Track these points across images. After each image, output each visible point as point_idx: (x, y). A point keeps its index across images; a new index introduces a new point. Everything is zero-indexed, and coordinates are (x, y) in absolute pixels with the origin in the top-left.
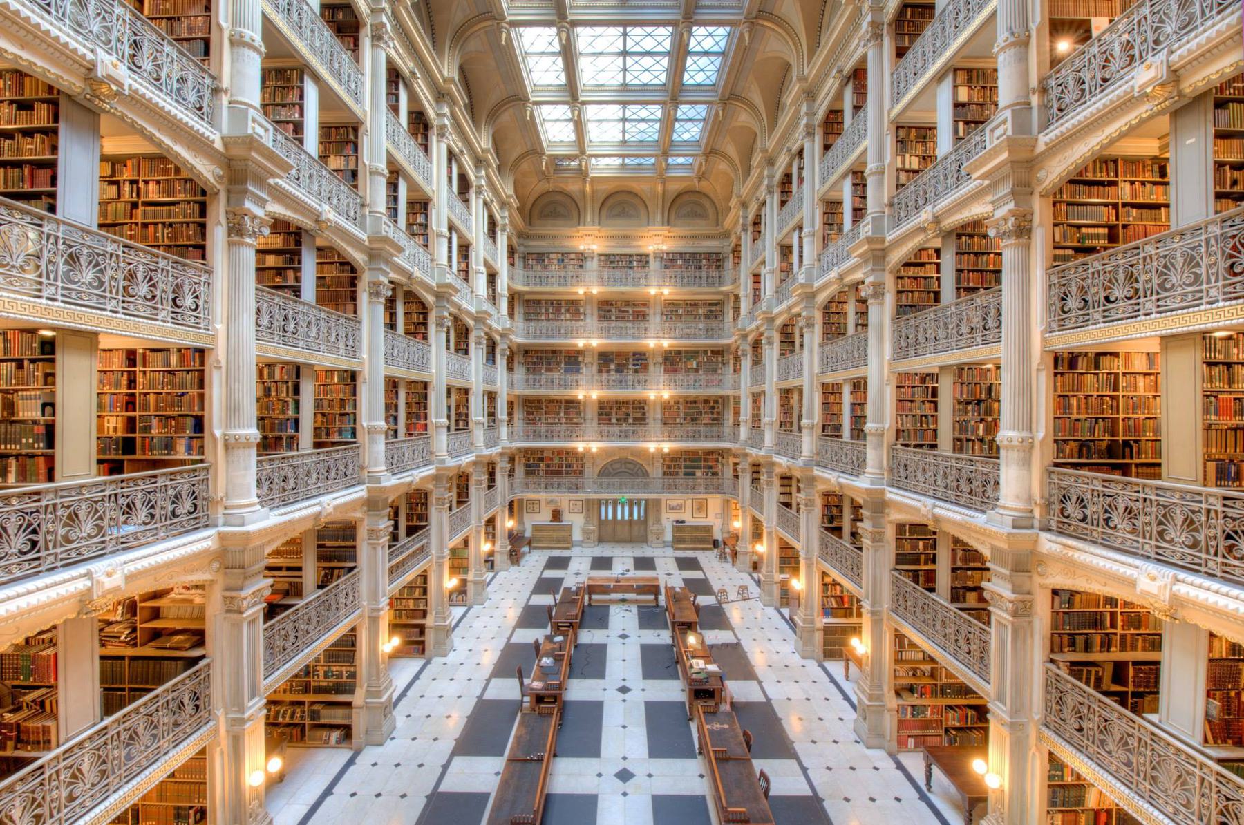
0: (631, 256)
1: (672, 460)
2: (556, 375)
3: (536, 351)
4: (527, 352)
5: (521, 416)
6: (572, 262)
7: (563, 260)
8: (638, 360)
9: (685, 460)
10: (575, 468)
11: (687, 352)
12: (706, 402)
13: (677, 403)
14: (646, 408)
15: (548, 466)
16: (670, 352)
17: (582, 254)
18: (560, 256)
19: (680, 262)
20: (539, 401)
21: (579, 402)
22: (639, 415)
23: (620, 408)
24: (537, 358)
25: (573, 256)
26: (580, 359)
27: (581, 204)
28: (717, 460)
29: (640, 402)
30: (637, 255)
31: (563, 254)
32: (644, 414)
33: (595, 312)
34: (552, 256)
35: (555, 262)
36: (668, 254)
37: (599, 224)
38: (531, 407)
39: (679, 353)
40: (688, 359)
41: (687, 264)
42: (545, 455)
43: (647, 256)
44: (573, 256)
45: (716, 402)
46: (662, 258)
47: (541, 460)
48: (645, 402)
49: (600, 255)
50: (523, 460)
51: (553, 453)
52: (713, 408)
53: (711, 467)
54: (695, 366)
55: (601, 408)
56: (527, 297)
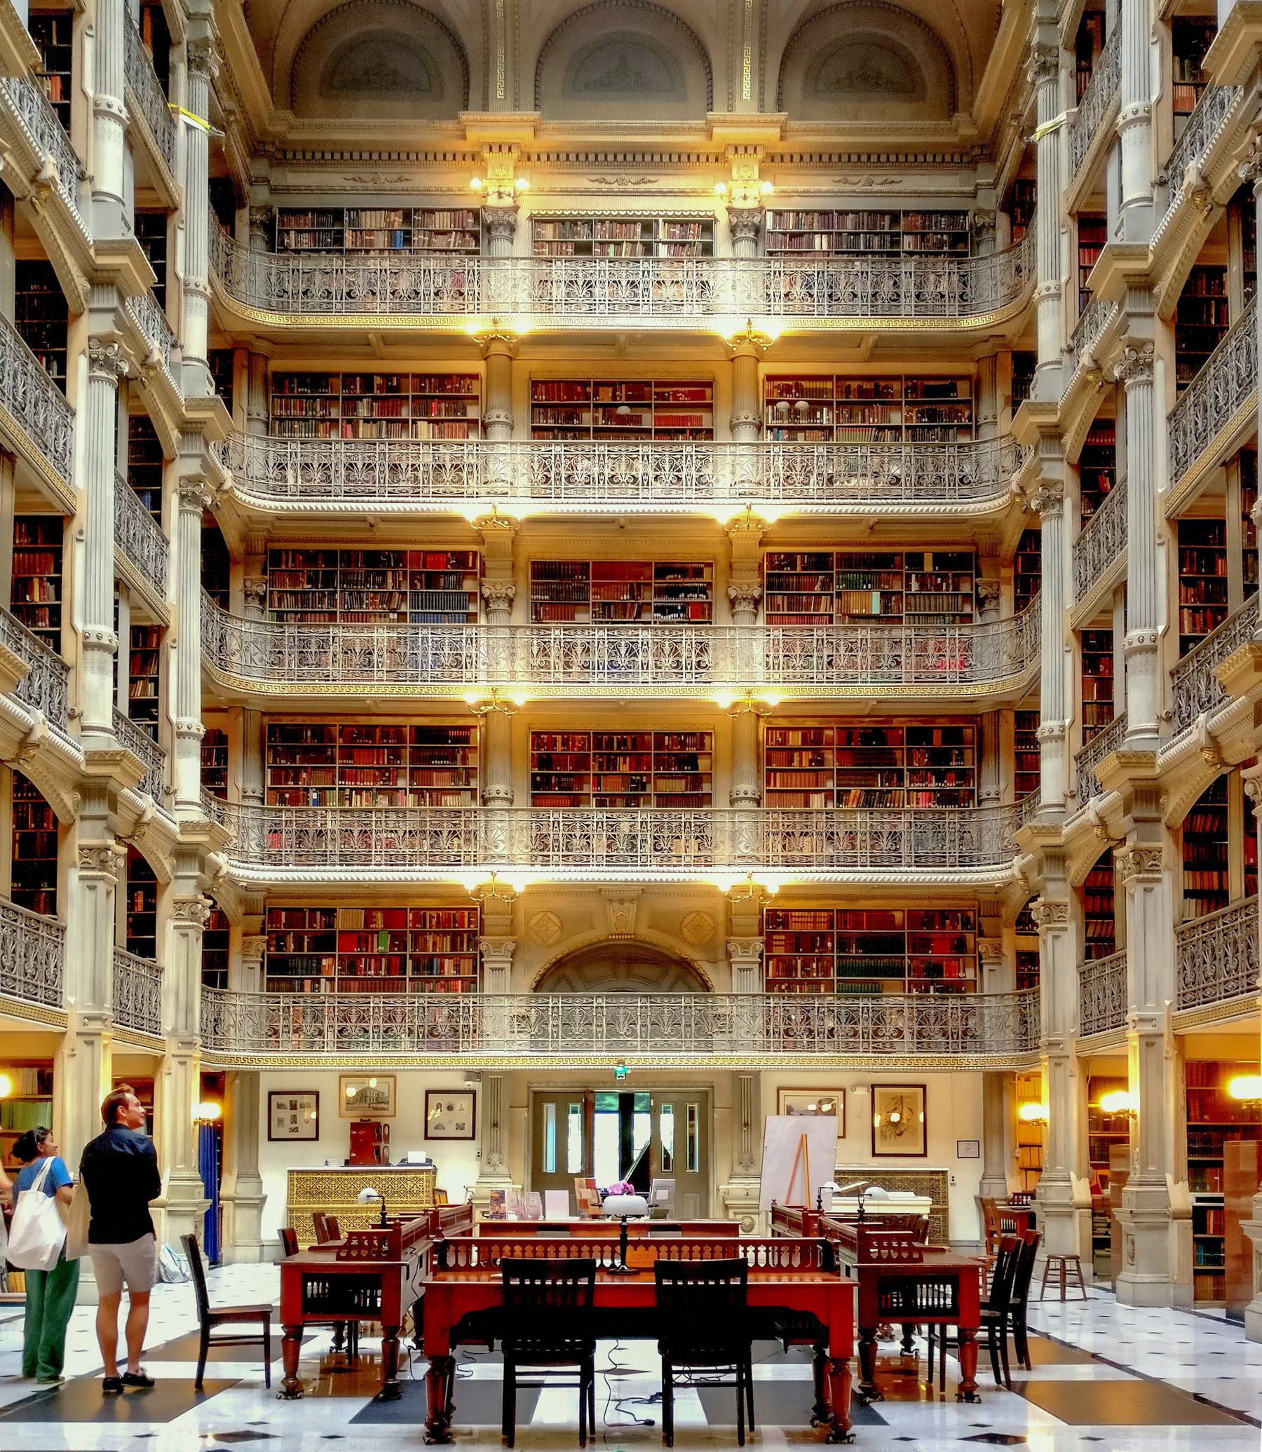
0: (648, 227)
1: (801, 941)
2: (381, 635)
3: (311, 557)
4: (275, 557)
5: (254, 786)
6: (439, 242)
7: (408, 241)
8: (673, 591)
9: (843, 945)
10: (449, 971)
11: (847, 560)
12: (919, 735)
13: (813, 738)
14: (703, 764)
15: (351, 965)
16: (790, 559)
17: (476, 214)
18: (397, 220)
19: (821, 243)
20: (321, 732)
21: (462, 735)
22: (679, 786)
23: (610, 762)
24: (312, 580)
25: (442, 221)
26: (469, 586)
27: (471, 41)
28: (960, 946)
29: (681, 738)
30: (671, 222)
31: (407, 215)
32: (697, 780)
33: (523, 415)
34: (368, 221)
35: (381, 240)
36: (778, 213)
37: (537, 107)
38: (290, 755)
39: (820, 561)
40: (852, 585)
41: (847, 249)
42: (340, 924)
43: (707, 226)
44: (442, 221)
45: (952, 735)
46: (758, 230)
47: (325, 942)
48: (700, 738)
49: (539, 221)
50: (260, 942)
51: (369, 915)
52: (940, 757)
53: (935, 969)
54: (876, 609)
55: (542, 762)
56: (276, 365)
